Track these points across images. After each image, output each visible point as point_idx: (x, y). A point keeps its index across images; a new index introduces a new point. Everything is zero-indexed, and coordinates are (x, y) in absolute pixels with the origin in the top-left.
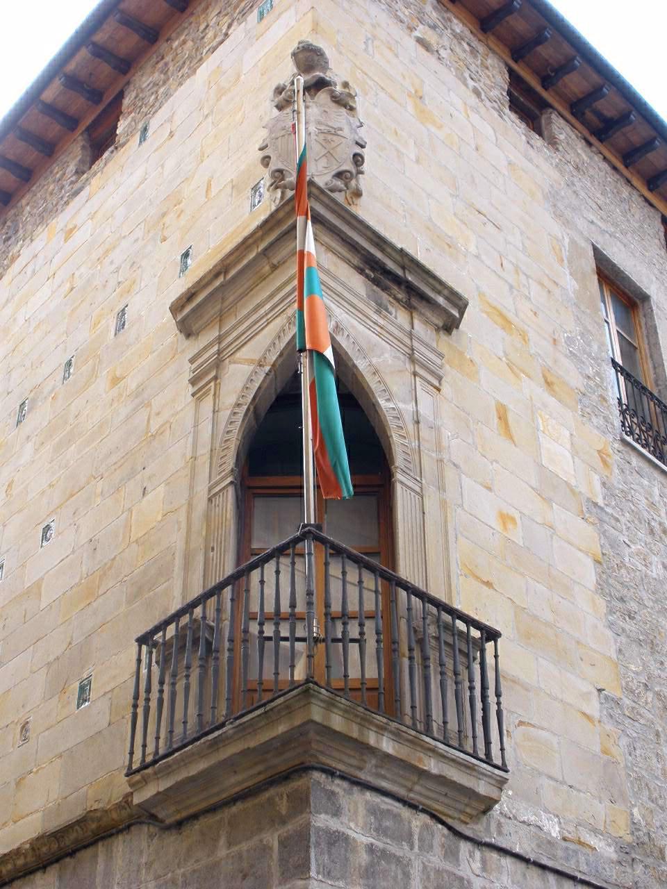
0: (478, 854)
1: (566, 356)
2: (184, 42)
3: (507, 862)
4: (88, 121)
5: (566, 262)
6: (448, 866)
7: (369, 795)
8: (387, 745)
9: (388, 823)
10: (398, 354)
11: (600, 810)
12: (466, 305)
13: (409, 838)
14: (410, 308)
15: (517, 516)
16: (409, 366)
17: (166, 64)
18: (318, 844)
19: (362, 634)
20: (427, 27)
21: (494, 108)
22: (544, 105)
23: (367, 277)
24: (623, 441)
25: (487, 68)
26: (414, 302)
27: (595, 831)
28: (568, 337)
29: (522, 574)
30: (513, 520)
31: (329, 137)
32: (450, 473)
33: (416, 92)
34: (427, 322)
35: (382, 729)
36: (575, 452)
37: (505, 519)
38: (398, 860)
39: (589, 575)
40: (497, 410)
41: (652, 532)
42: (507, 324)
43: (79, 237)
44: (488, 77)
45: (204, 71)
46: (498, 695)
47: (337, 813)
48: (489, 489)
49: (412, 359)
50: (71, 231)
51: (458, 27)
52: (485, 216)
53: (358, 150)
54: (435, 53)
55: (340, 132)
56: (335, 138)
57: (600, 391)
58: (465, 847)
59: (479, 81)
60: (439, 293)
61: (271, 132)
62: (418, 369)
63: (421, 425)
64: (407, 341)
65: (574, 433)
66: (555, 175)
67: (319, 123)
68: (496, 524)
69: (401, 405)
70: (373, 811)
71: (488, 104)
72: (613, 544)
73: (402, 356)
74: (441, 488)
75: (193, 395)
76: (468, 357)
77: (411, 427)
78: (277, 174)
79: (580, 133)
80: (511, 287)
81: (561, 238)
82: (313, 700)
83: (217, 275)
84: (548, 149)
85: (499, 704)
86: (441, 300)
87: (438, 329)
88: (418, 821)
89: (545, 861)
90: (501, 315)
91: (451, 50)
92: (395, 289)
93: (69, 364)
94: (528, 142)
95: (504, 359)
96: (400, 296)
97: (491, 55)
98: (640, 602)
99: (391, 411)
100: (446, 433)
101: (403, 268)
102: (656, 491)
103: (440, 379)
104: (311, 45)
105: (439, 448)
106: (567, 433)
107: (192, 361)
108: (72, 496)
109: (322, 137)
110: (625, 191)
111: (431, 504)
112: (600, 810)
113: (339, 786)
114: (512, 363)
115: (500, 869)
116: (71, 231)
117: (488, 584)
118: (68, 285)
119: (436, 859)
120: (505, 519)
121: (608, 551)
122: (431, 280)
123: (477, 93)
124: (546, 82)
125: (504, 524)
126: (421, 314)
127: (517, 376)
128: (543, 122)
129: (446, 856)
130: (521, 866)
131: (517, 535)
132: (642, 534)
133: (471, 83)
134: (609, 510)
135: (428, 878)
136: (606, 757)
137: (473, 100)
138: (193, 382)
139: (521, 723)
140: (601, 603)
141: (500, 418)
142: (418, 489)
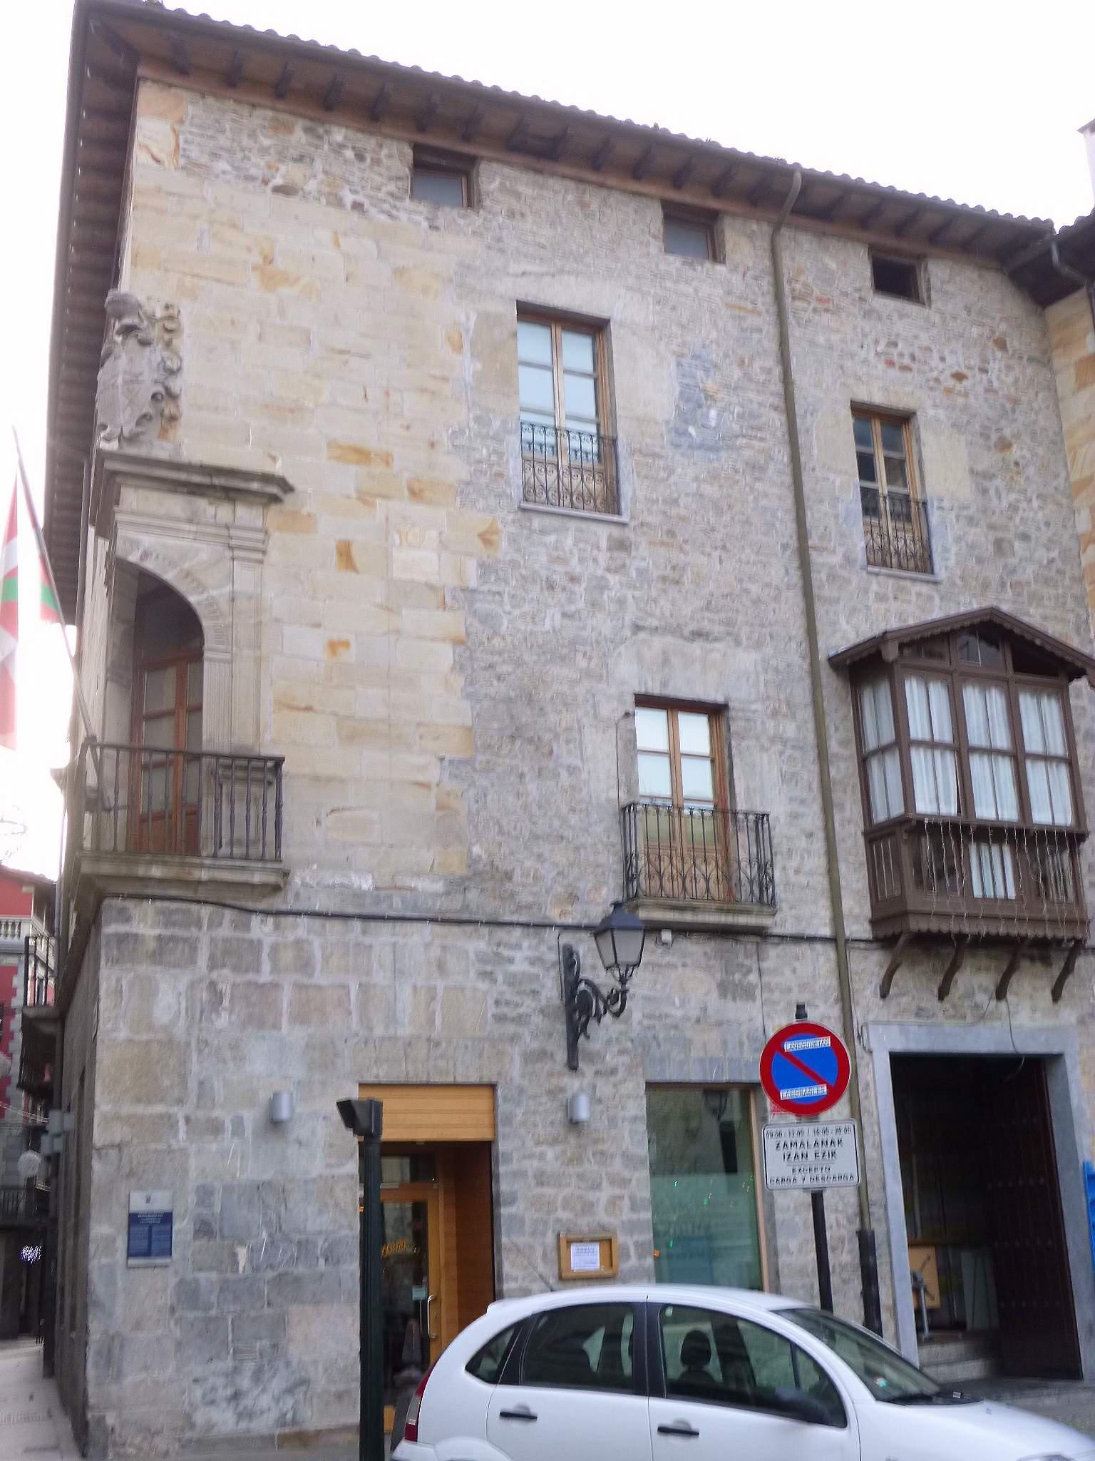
0: (271, 920)
3: (303, 921)
5: (466, 346)
6: (239, 934)
7: (159, 904)
8: (156, 872)
9: (175, 917)
11: (427, 857)
13: (199, 924)
16: (228, 554)
18: (108, 944)
20: (291, 164)
22: (473, 160)
24: (524, 510)
26: (232, 494)
27: (418, 875)
30: (346, 644)
33: (265, 258)
35: (150, 863)
36: (443, 545)
38: (185, 940)
39: (446, 655)
41: (551, 587)
47: (127, 920)
49: (231, 548)
51: (338, 135)
57: (496, 469)
58: (255, 920)
62: (237, 553)
64: (225, 532)
69: (215, 593)
70: (161, 912)
71: (373, 211)
72: (486, 619)
88: (206, 912)
89: (350, 910)
97: (388, 142)
98: (519, 663)
102: (569, 542)
105: (258, 611)
110: (594, 198)
112: (427, 857)
113: (130, 904)
115: (295, 927)
117: (308, 709)
119: (225, 931)
121: (477, 626)
123: (357, 206)
129: (236, 928)
130: (317, 922)
132: (535, 591)
134: (485, 588)
135: (216, 946)
136: (441, 813)
137: (355, 216)
140: (459, 681)
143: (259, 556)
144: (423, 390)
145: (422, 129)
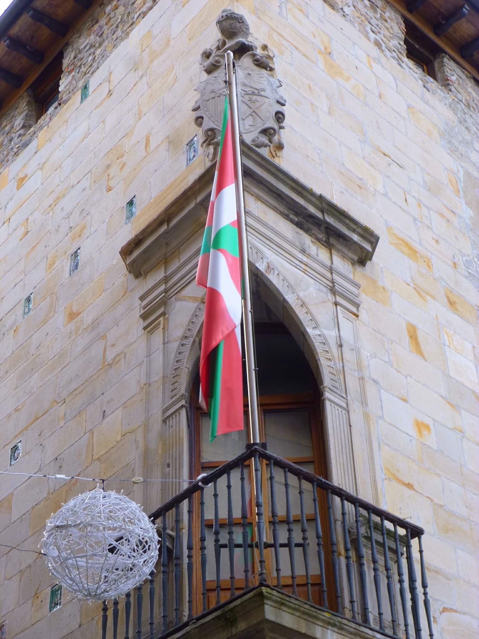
1: (466, 277)
2: (116, 8)
4: (33, 78)
10: (322, 287)
12: (377, 239)
14: (329, 246)
15: (430, 423)
16: (330, 297)
17: (101, 27)
19: (304, 539)
21: (393, 57)
22: (437, 51)
23: (292, 221)
25: (386, 21)
26: (332, 240)
28: (466, 260)
29: (439, 476)
30: (427, 427)
31: (254, 97)
32: (371, 389)
33: (325, 49)
34: (344, 256)
37: (421, 426)
40: (408, 330)
42: (413, 253)
43: (31, 185)
44: (387, 28)
45: (137, 33)
46: (424, 586)
48: (405, 401)
49: (333, 291)
50: (22, 179)
52: (390, 157)
53: (279, 108)
54: (340, 11)
55: (262, 93)
56: (259, 98)
59: (379, 33)
60: (354, 231)
61: (202, 94)
62: (339, 299)
63: (344, 348)
64: (329, 275)
65: (476, 346)
66: (447, 113)
67: (244, 85)
68: (413, 432)
69: (326, 332)
71: (388, 53)
73: (325, 289)
74: (364, 402)
75: (145, 328)
76: (381, 285)
77: (335, 350)
78: (210, 133)
79: (469, 73)
80: (415, 220)
81: (457, 171)
82: (265, 601)
83: (161, 224)
84: (441, 91)
85: (425, 594)
86: (355, 237)
87: (353, 263)
90: (407, 245)
91: (354, 6)
92: (315, 230)
93: (28, 300)
94: (424, 86)
95: (411, 284)
96: (320, 236)
97: (388, 8)
99: (318, 338)
100: (365, 353)
101: (322, 212)
103: (357, 306)
104: (234, 13)
105: (360, 366)
106: (470, 346)
107: (142, 298)
108: (37, 419)
109: (247, 98)
111: (356, 417)
114: (418, 287)
116: (22, 179)
117: (409, 486)
118: (22, 230)
120: (421, 426)
122: (347, 221)
123: (377, 44)
124: (437, 29)
125: (420, 432)
126: (338, 251)
127: (425, 300)
128: (436, 65)
131: (431, 440)
133: (372, 36)
137: (375, 52)
138: (144, 317)
139: (445, 610)
141: (411, 337)
142: (344, 405)
143: (354, 309)
144: (442, 215)
145: (410, 11)
